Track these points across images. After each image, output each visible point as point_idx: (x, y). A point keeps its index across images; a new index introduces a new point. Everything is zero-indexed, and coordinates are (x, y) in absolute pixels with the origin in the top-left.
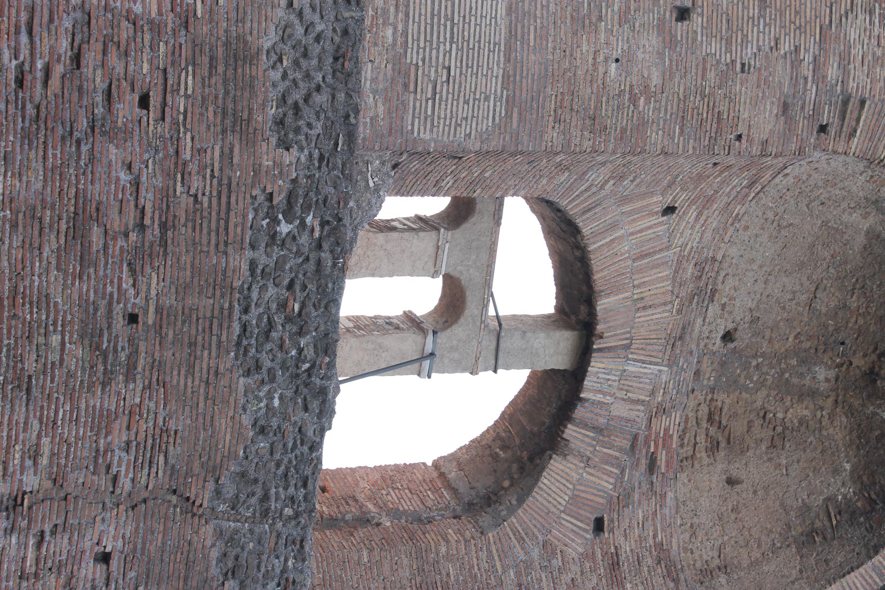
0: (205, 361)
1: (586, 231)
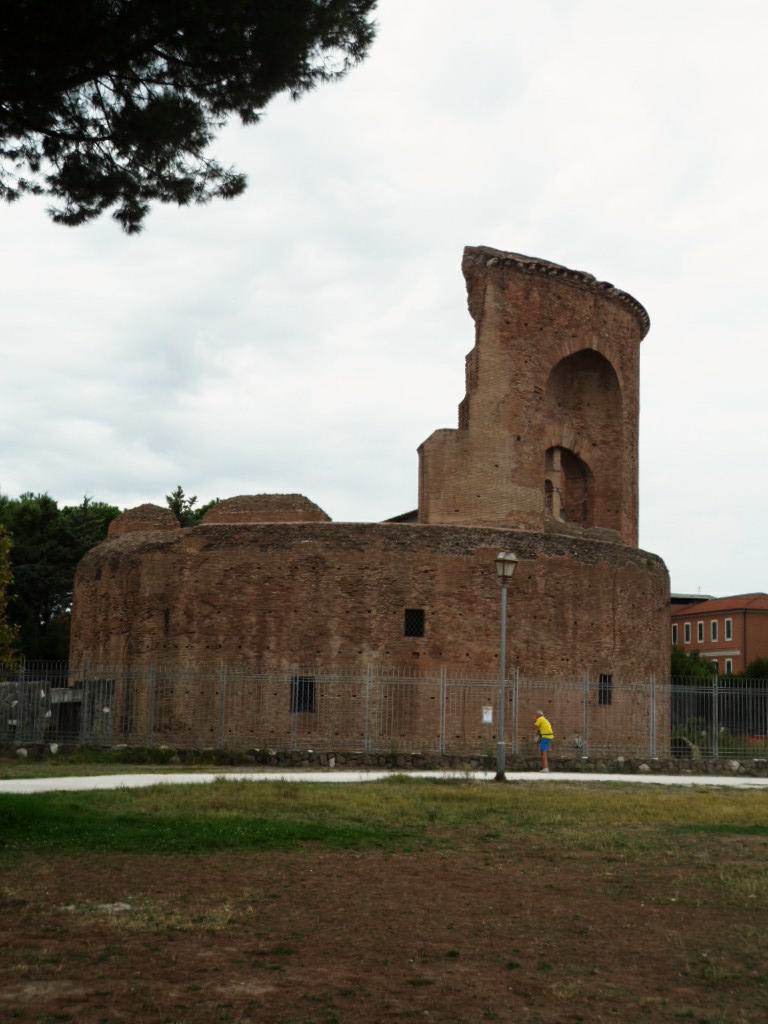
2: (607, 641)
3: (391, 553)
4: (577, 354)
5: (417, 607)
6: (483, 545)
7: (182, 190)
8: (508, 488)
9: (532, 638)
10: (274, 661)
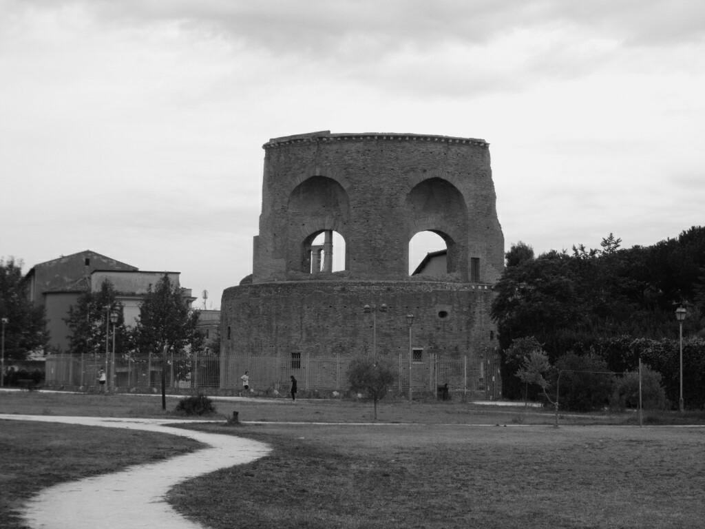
1: (307, 236)
2: (296, 335)
4: (306, 181)
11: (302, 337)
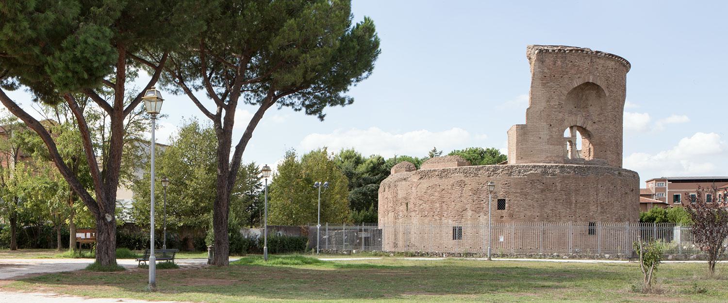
0: (587, 179)
3: (491, 177)
5: (503, 198)
6: (532, 172)
7: (342, 102)
8: (547, 147)
9: (554, 208)
10: (446, 221)
11: (597, 210)
